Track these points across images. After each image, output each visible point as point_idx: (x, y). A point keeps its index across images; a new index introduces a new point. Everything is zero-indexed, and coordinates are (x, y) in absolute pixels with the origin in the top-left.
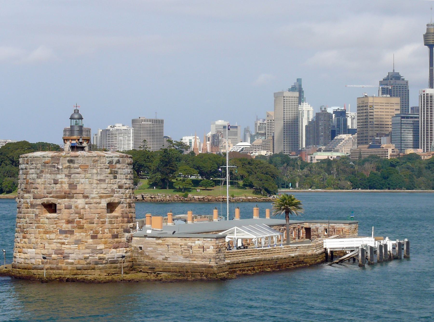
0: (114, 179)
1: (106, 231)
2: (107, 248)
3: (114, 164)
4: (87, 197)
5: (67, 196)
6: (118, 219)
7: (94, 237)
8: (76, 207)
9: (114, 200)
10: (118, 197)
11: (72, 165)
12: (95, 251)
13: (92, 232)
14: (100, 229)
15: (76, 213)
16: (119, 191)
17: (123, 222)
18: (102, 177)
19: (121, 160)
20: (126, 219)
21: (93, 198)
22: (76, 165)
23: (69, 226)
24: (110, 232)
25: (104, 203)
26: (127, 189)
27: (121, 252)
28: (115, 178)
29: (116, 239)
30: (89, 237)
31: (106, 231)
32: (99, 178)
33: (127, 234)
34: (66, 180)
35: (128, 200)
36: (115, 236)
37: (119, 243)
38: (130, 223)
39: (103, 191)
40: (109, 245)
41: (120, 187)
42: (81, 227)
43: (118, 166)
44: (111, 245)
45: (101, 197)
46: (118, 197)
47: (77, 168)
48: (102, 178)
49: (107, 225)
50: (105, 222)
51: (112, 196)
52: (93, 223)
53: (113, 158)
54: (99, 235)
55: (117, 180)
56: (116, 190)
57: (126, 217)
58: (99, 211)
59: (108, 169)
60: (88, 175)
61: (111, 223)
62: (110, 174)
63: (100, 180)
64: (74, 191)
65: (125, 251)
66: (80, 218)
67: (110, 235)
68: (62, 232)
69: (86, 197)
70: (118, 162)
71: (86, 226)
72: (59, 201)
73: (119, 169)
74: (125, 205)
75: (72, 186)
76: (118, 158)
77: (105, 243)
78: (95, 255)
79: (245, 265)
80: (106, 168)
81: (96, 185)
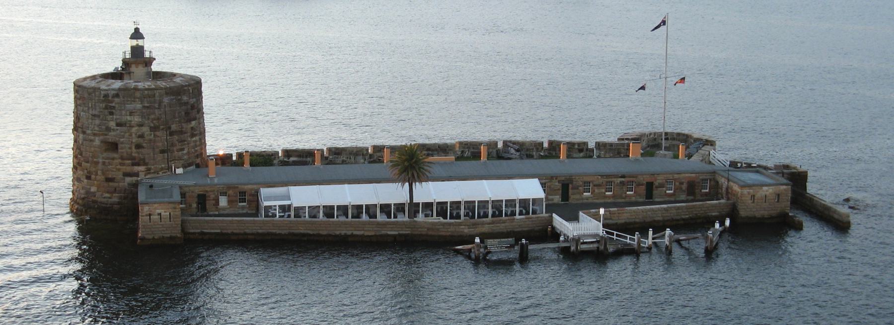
1: (99, 172)
7: (88, 178)
17: (121, 164)
21: (89, 135)
25: (97, 142)
31: (99, 172)
32: (94, 112)
36: (109, 180)
38: (139, 165)
41: (118, 125)
43: (116, 100)
45: (95, 135)
49: (100, 166)
54: (93, 177)
61: (104, 163)
63: (94, 116)
69: (84, 133)
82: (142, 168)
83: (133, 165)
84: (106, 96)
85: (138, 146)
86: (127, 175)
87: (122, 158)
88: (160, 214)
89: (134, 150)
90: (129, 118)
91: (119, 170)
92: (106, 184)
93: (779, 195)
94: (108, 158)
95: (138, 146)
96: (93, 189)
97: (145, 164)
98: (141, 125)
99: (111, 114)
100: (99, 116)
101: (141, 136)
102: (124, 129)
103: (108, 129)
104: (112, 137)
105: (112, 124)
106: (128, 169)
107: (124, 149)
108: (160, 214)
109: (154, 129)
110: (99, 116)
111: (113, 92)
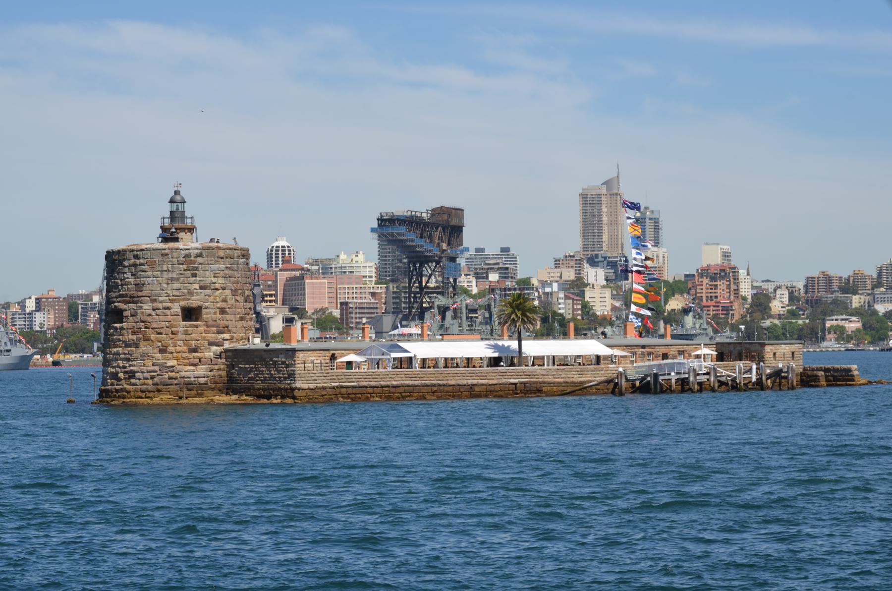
4: (154, 301)
5: (133, 299)
7: (162, 351)
8: (142, 313)
11: (138, 262)
12: (163, 367)
13: (160, 344)
14: (171, 341)
15: (142, 322)
17: (207, 332)
19: (204, 253)
21: (161, 302)
22: (142, 261)
23: (134, 337)
24: (185, 345)
25: (176, 308)
30: (157, 350)
32: (170, 275)
33: (214, 348)
34: (132, 280)
35: (219, 305)
41: (202, 288)
42: (147, 339)
43: (200, 260)
47: (143, 264)
49: (181, 336)
52: (161, 334)
54: (171, 349)
55: (198, 278)
57: (213, 326)
58: (170, 318)
60: (155, 273)
63: (172, 279)
64: (140, 294)
66: (146, 328)
67: (185, 348)
68: (127, 345)
71: (153, 337)
72: (125, 307)
75: (139, 286)
79: (393, 390)
81: (165, 286)
82: (227, 336)
83: (219, 332)
84: (187, 256)
85: (223, 311)
86: (211, 344)
87: (208, 326)
88: (312, 362)
90: (214, 280)
91: (204, 338)
93: (793, 353)
94: (191, 326)
95: (223, 311)
96: (170, 363)
97: (229, 332)
98: (224, 289)
99: (194, 275)
100: (178, 279)
101: (225, 301)
102: (208, 292)
103: (191, 293)
104: (194, 302)
105: (197, 286)
106: (212, 337)
107: (207, 315)
108: (312, 362)
109: (234, 292)
110: (178, 279)
111: (196, 251)
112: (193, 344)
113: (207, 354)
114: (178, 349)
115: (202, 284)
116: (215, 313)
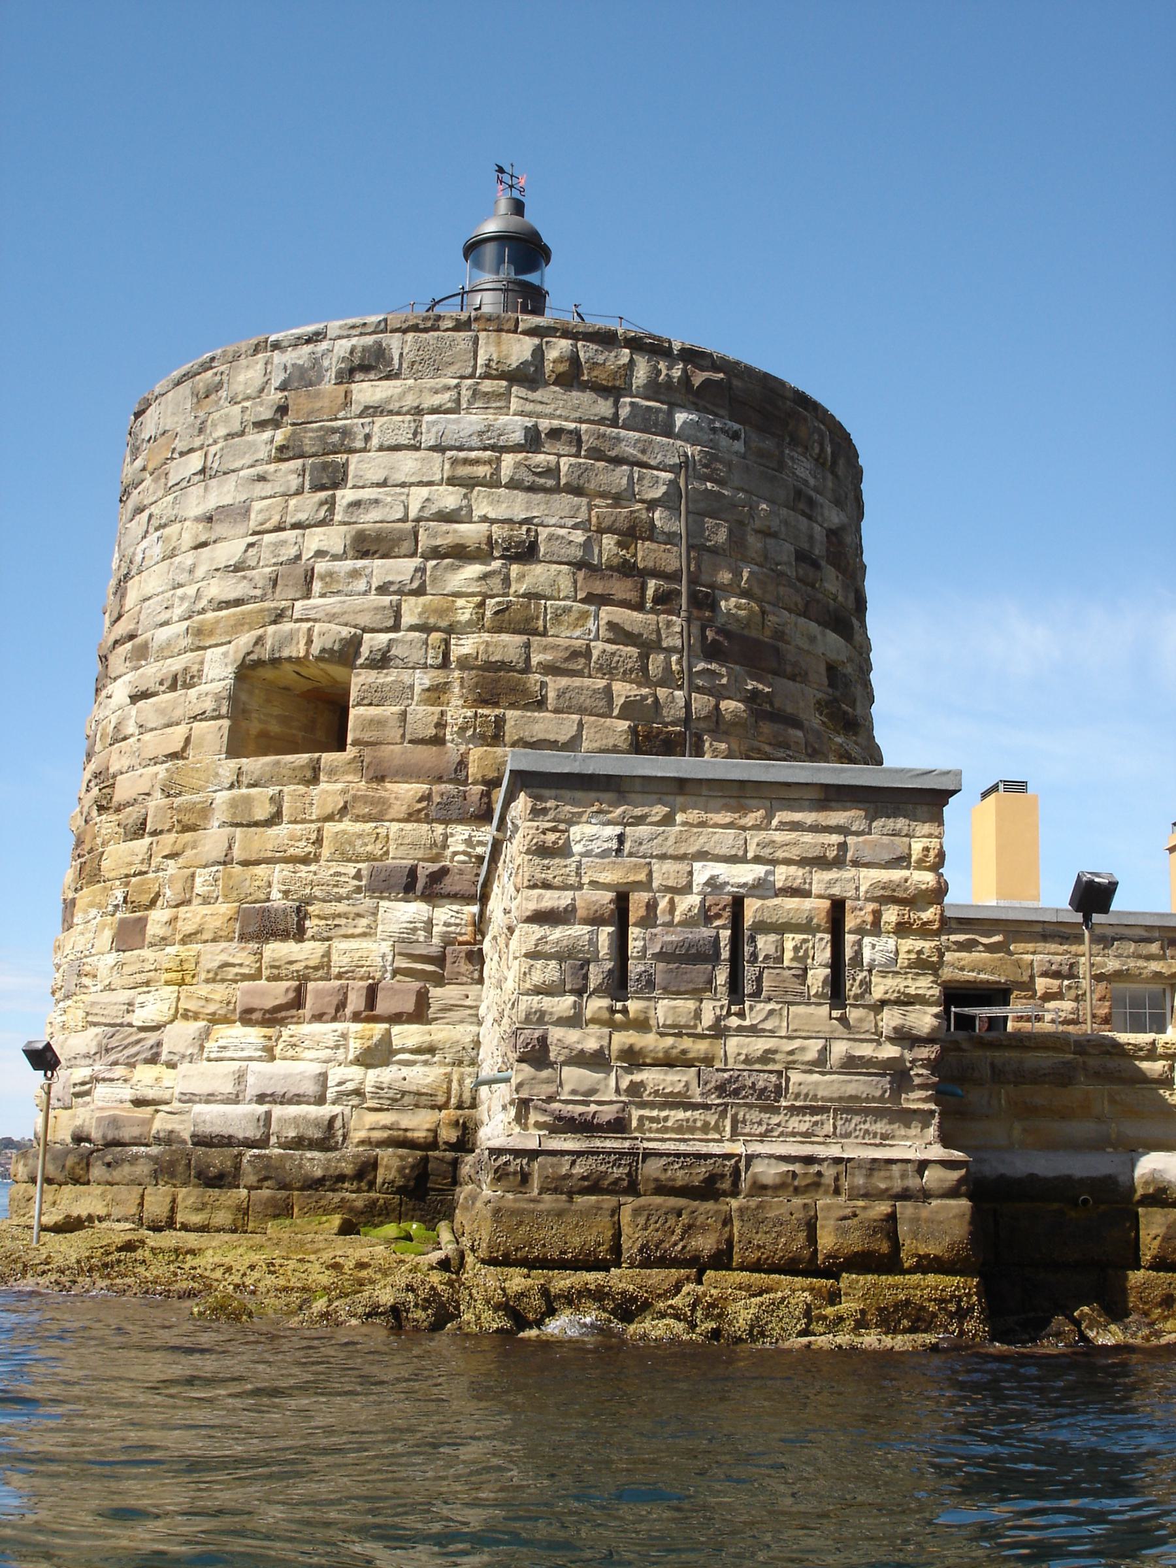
0: (318, 487)
2: (196, 1017)
3: (328, 385)
6: (323, 786)
9: (291, 637)
10: (331, 618)
16: (355, 574)
18: (224, 493)
20: (405, 792)
26: (460, 554)
27: (319, 1054)
28: (331, 478)
29: (276, 950)
33: (404, 913)
35: (465, 646)
37: (303, 979)
39: (220, 589)
40: (204, 990)
41: (367, 546)
43: (367, 391)
44: (220, 992)
46: (331, 618)
48: (227, 500)
50: (206, 811)
51: (279, 617)
53: (324, 345)
55: (345, 496)
56: (321, 566)
57: (407, 774)
59: (276, 424)
62: (283, 453)
65: (355, 1047)
70: (370, 363)
73: (373, 411)
74: (422, 680)
76: (369, 340)
77: (182, 977)
78: (119, 1071)
80: (261, 425)
85: (496, 685)
89: (457, 711)
92: (240, 955)
104: (312, 627)
112: (276, 885)
113: (344, 952)
114: (193, 916)
115: (369, 519)
116: (436, 693)
